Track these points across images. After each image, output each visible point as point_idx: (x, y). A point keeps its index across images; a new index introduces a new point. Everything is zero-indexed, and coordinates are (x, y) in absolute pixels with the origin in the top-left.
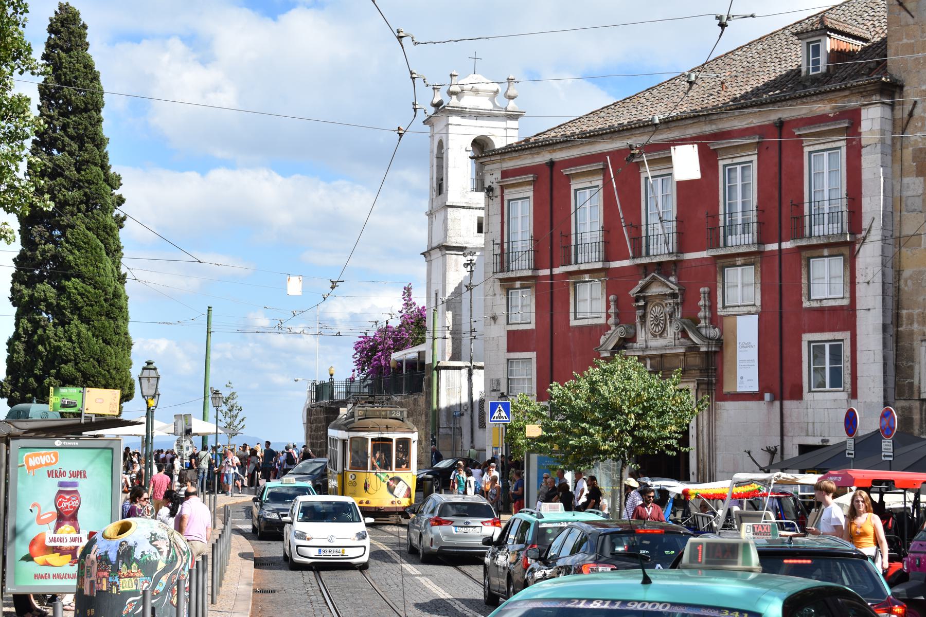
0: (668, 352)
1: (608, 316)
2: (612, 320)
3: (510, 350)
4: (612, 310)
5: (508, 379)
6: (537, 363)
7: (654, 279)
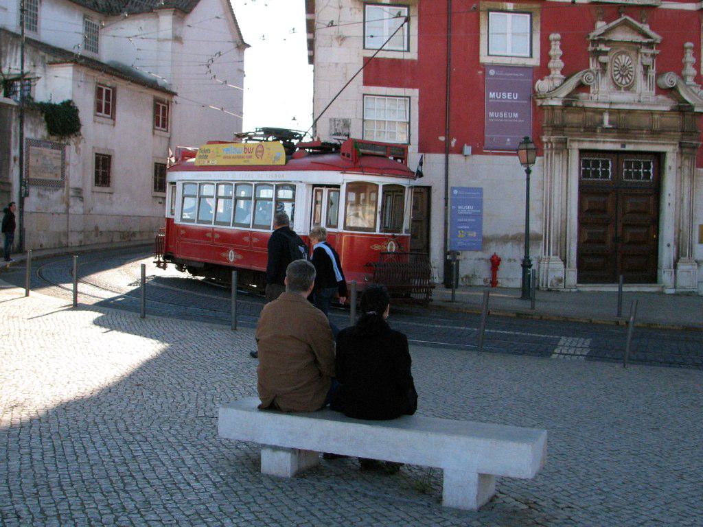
0: (640, 107)
1: (545, 57)
2: (556, 64)
3: (367, 82)
4: (556, 50)
5: (363, 120)
6: (420, 103)
7: (625, 23)
